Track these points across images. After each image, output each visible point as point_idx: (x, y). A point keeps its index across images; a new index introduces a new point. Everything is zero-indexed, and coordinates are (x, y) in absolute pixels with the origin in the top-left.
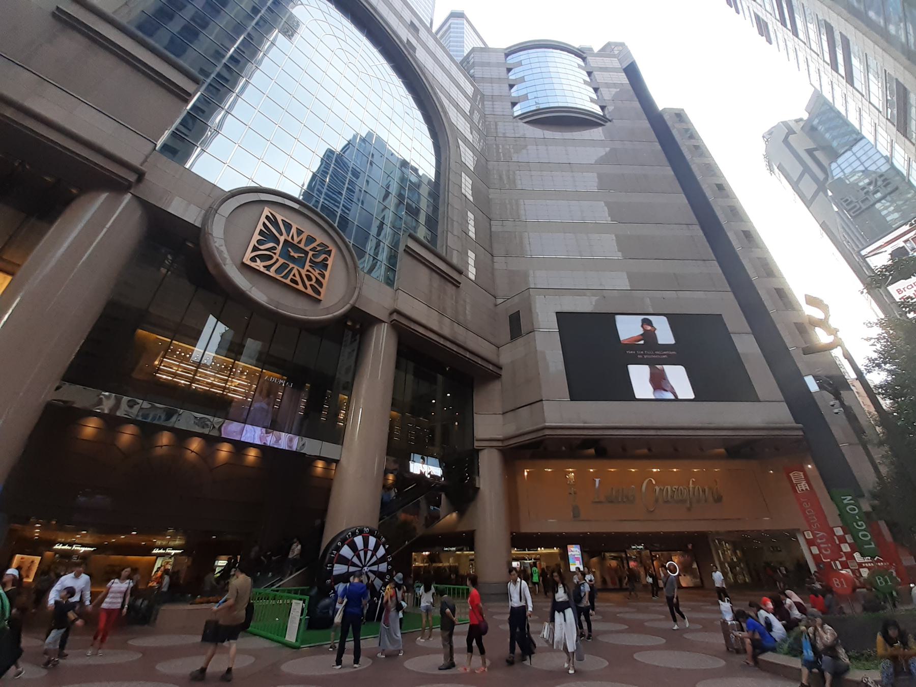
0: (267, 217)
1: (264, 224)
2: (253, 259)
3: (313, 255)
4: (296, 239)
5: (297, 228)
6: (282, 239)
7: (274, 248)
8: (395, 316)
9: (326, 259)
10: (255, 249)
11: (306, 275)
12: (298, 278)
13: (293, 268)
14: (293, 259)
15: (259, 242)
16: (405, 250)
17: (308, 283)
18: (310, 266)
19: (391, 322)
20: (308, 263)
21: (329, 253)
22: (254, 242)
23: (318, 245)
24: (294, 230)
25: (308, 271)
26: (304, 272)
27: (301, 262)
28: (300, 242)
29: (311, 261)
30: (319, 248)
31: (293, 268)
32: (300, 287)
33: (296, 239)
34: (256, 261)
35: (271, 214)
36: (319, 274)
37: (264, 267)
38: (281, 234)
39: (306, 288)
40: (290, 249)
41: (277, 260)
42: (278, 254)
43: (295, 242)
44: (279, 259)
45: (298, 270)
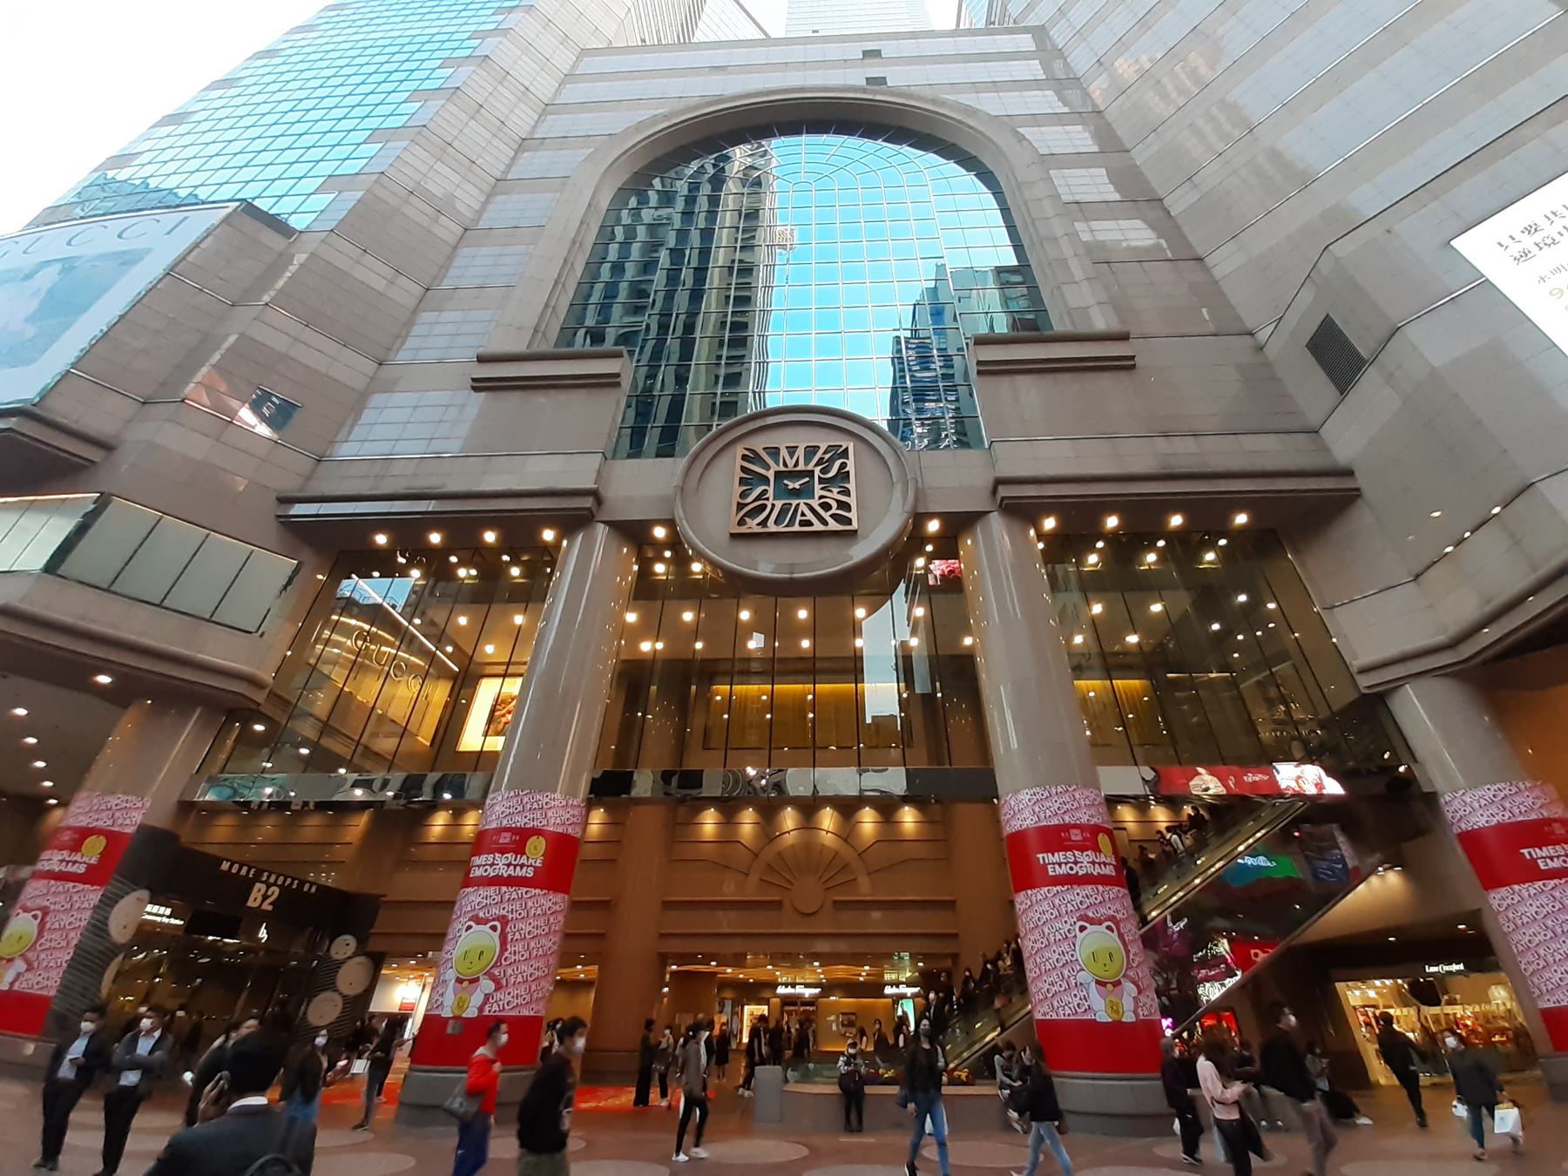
0: (744, 457)
1: (743, 469)
2: (741, 522)
3: (821, 471)
4: (791, 463)
5: (787, 447)
6: (771, 475)
8: (1004, 491)
9: (843, 465)
10: (740, 506)
11: (820, 505)
12: (810, 516)
13: (798, 504)
14: (796, 493)
15: (743, 495)
16: (979, 373)
17: (826, 515)
18: (822, 489)
19: (1000, 505)
20: (817, 486)
21: (845, 453)
22: (736, 499)
23: (825, 453)
24: (784, 453)
25: (821, 497)
26: (815, 503)
27: (806, 492)
28: (796, 464)
29: (821, 480)
30: (827, 456)
31: (798, 504)
32: (818, 526)
33: (791, 463)
34: (745, 523)
35: (746, 449)
36: (839, 493)
37: (758, 524)
38: (768, 467)
39: (825, 523)
40: (786, 482)
41: (773, 505)
42: (771, 498)
45: (806, 504)
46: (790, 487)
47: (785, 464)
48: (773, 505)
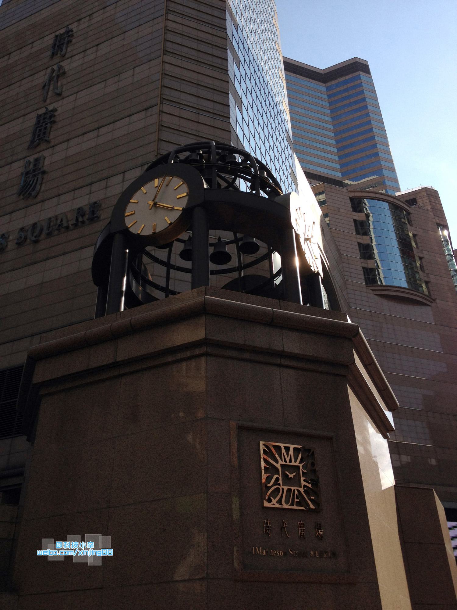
6: (278, 466)
7: (277, 479)
13: (294, 490)
20: (302, 479)
24: (283, 451)
28: (290, 461)
31: (294, 490)
38: (277, 462)
43: (288, 463)
44: (283, 487)
46: (290, 477)
47: (285, 461)
48: (283, 489)
